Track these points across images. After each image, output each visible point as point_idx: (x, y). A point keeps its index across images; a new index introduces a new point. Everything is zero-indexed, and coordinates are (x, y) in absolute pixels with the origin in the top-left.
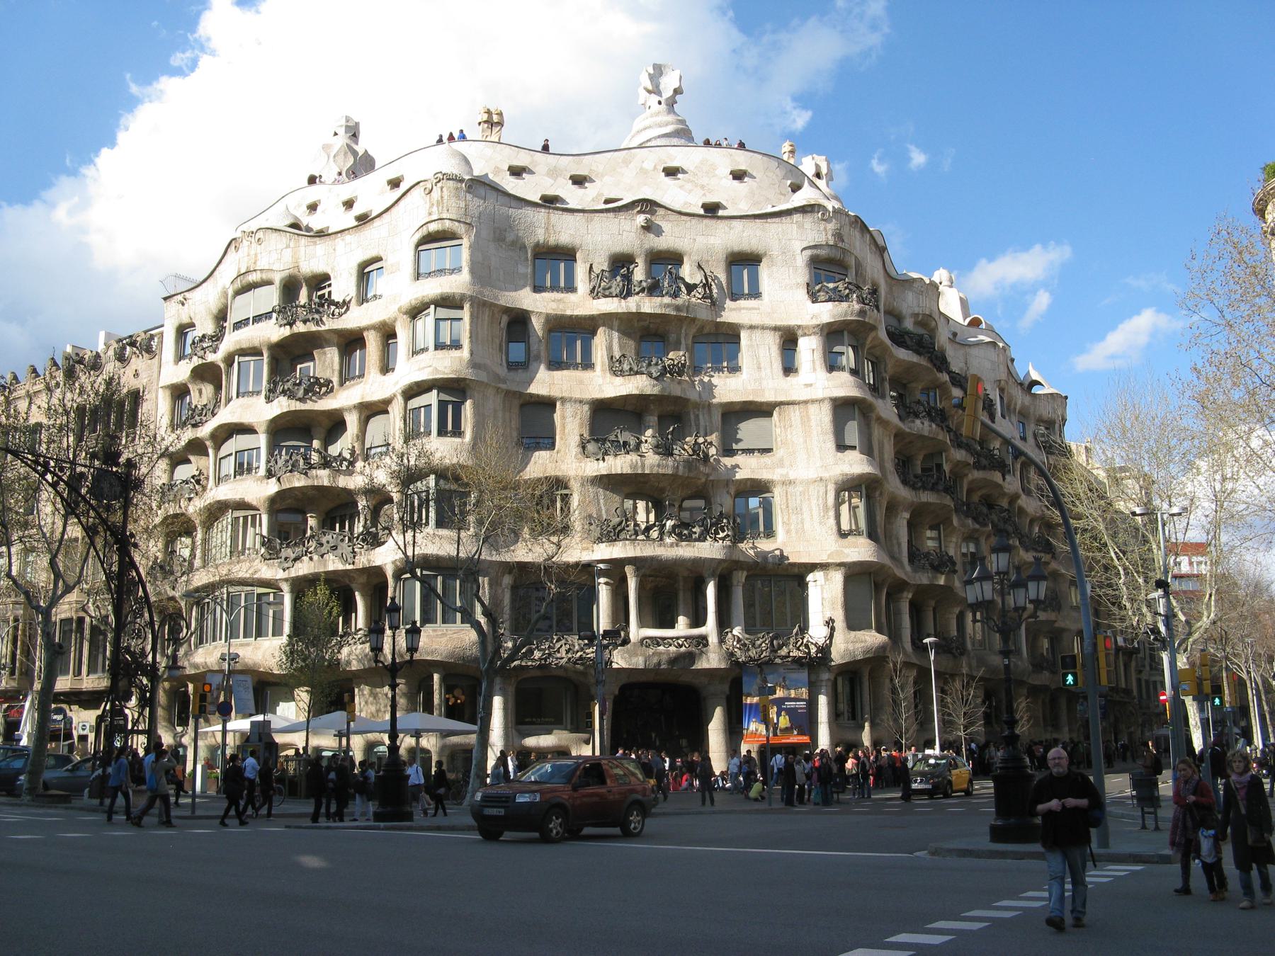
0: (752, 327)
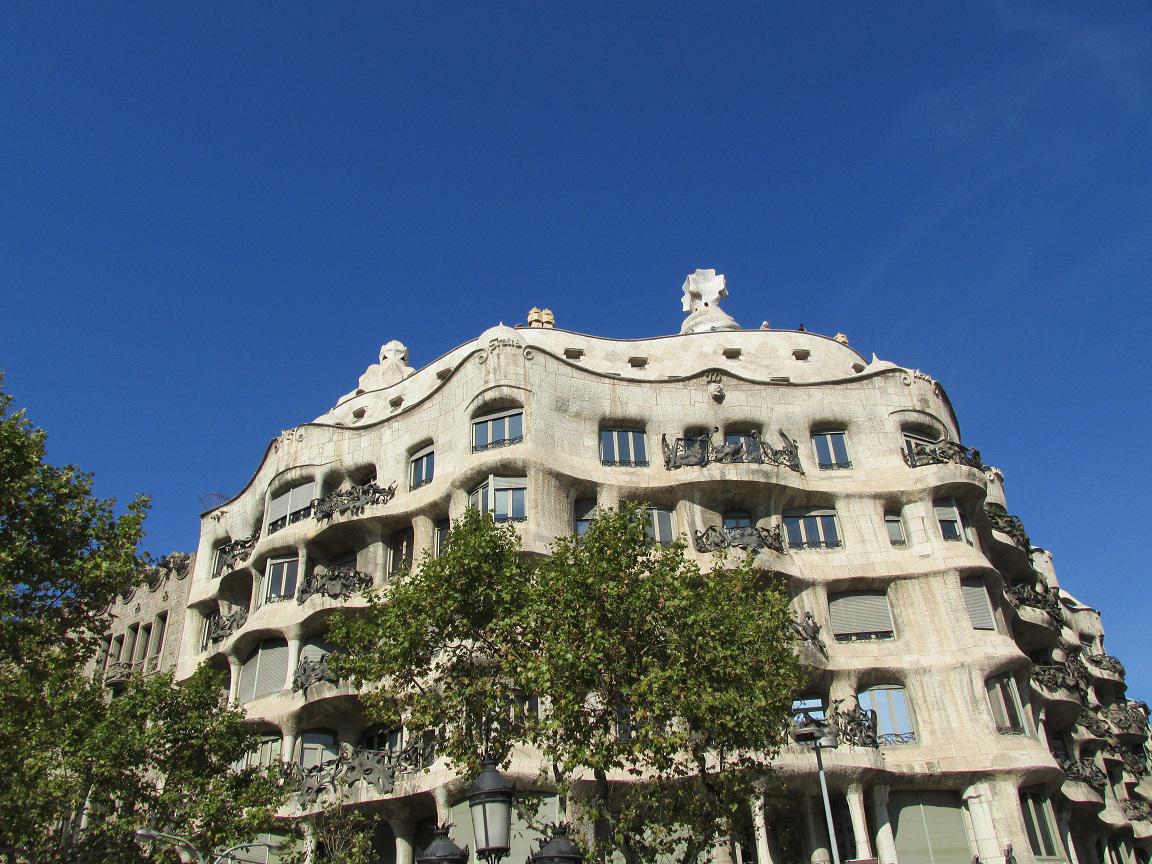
0: (848, 496)
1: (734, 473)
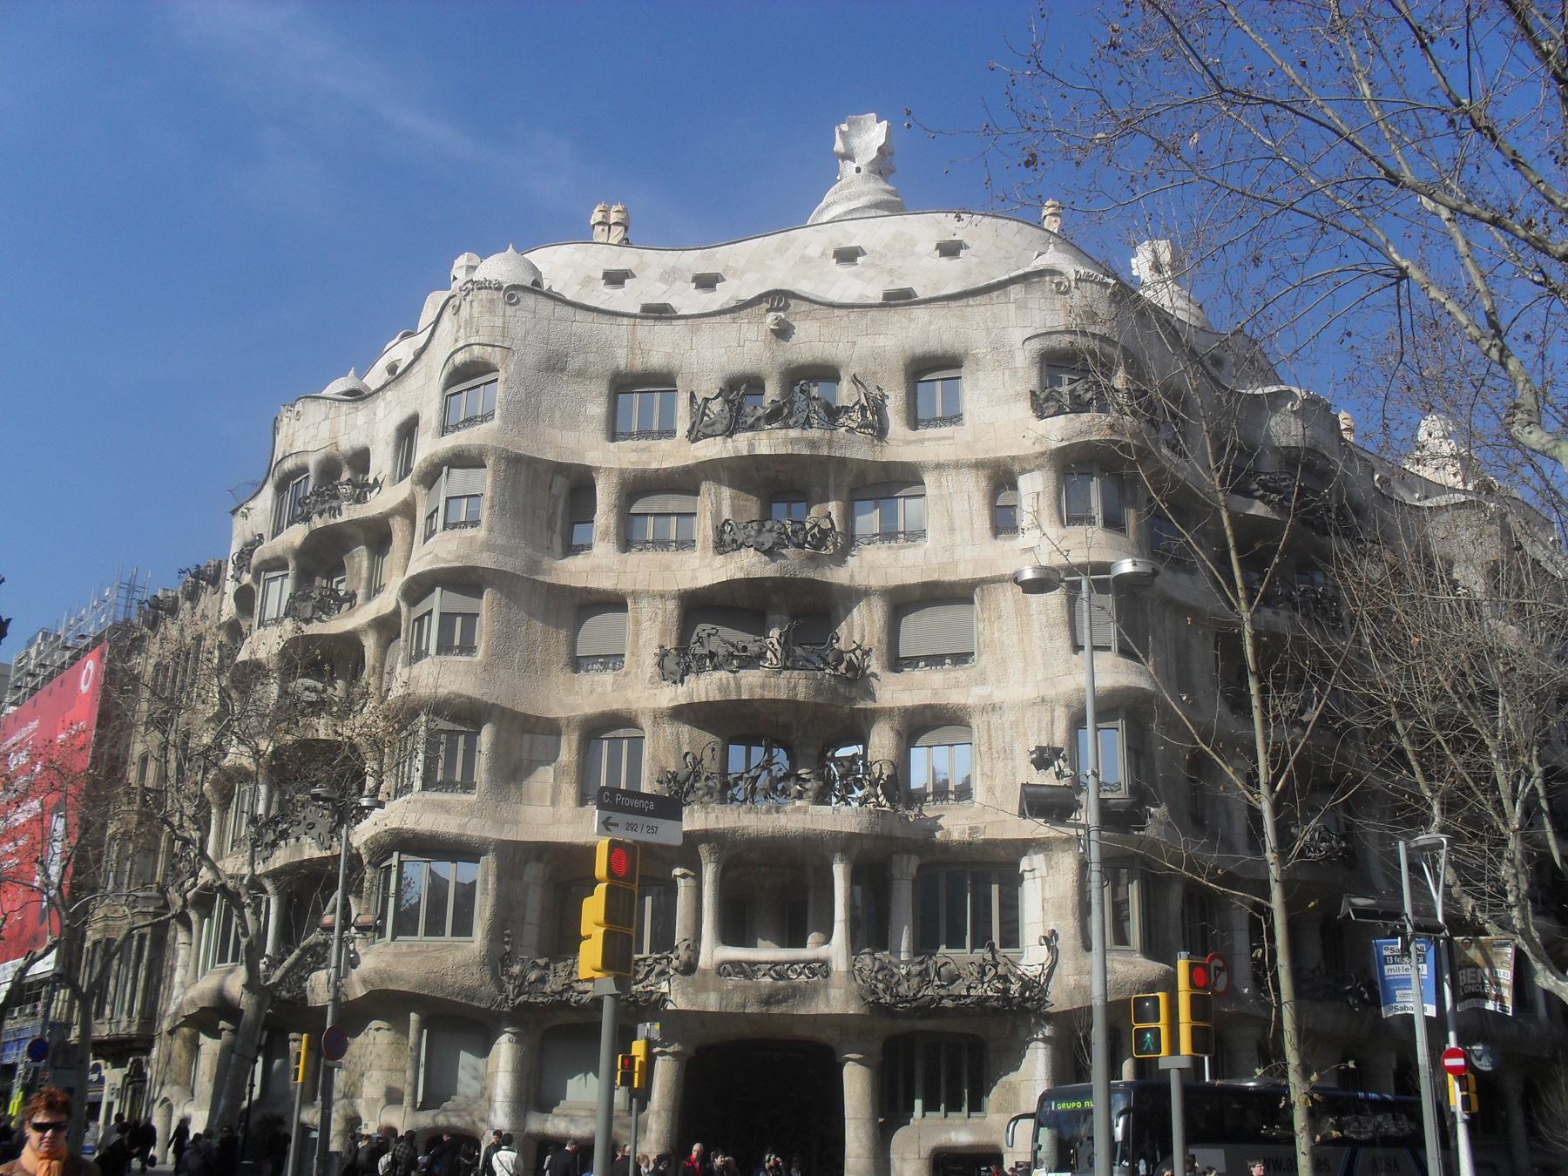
0: (939, 466)
1: (767, 443)
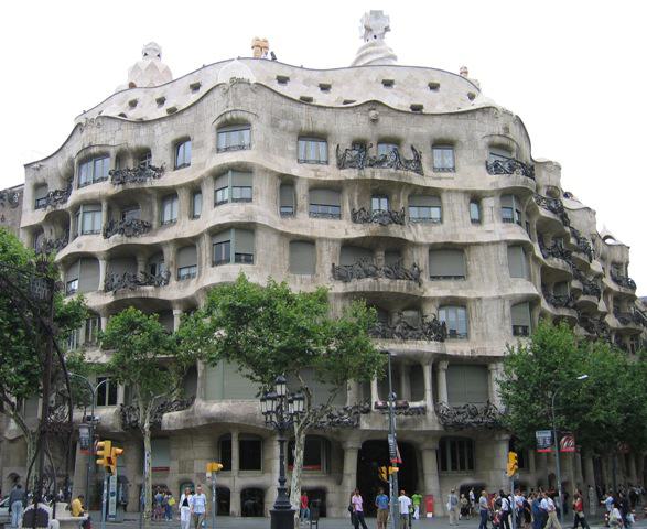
0: (449, 191)
1: (379, 174)
